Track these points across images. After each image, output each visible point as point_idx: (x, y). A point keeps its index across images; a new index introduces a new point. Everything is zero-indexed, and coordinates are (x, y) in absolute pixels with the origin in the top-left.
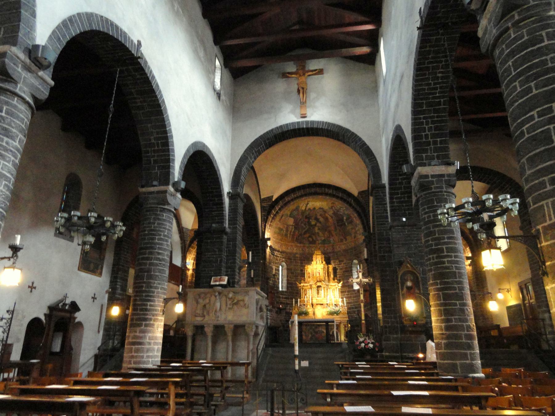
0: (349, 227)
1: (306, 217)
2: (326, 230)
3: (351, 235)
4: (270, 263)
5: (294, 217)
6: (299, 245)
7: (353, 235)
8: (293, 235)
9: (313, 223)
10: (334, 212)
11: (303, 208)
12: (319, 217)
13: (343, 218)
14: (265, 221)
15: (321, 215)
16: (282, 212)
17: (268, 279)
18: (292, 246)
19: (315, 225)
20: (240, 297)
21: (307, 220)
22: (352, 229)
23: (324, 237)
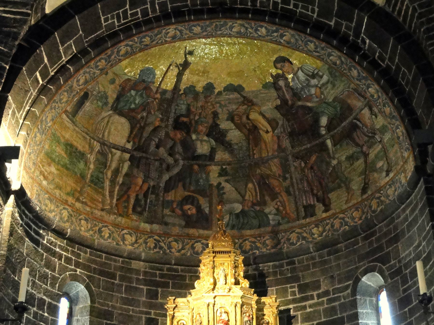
0: (340, 155)
1: (178, 125)
2: (248, 178)
3: (345, 183)
5: (129, 115)
6: (147, 227)
7: (356, 185)
8: (126, 188)
9: (203, 148)
10: (284, 101)
11: (169, 85)
12: (224, 125)
13: (317, 121)
15: (231, 118)
16: (81, 77)
18: (116, 225)
19: (211, 157)
21: (179, 135)
22: (351, 158)
23: (243, 201)
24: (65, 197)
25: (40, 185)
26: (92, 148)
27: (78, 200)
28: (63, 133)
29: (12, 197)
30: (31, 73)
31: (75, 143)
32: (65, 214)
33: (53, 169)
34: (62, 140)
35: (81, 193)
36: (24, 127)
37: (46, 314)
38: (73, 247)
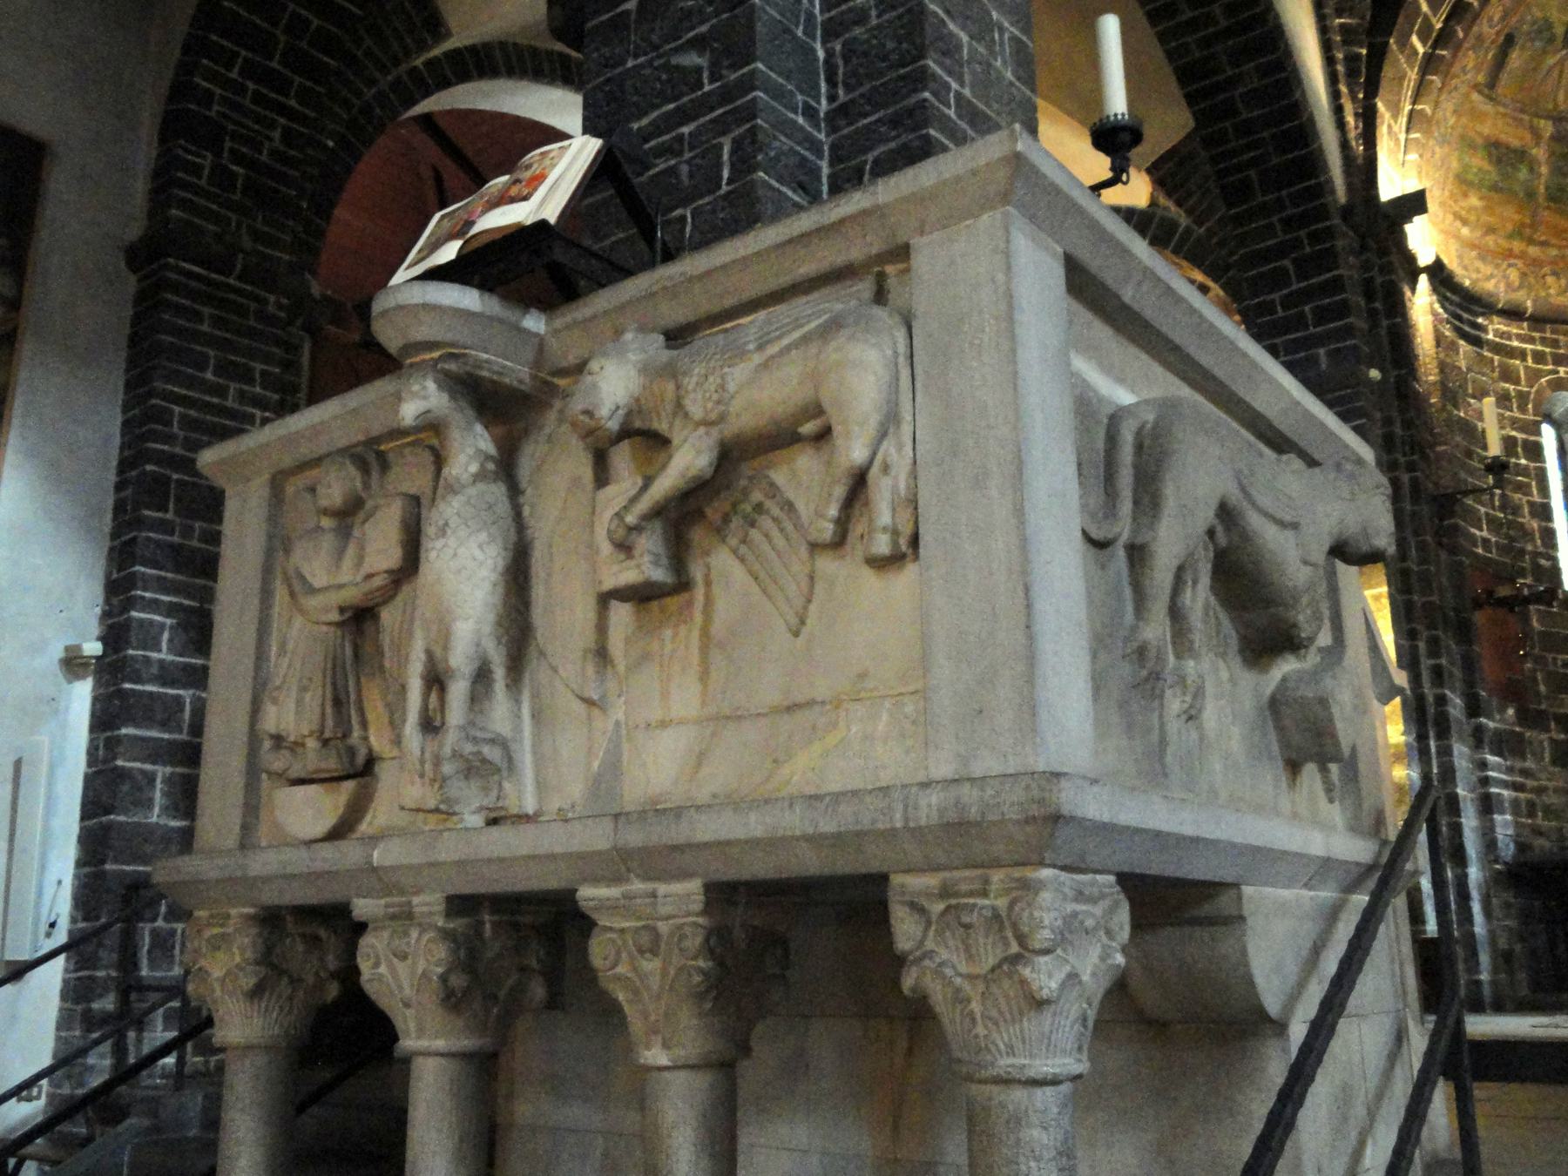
4: (1452, 396)
14: (1363, 73)
17: (1447, 504)
20: (747, 382)
24: (1504, 243)
25: (1457, 237)
26: (1536, 134)
27: (1531, 241)
28: (1479, 128)
29: (1423, 280)
30: (1404, 43)
31: (1503, 137)
32: (1514, 275)
33: (1474, 201)
34: (1479, 141)
35: (1533, 226)
36: (1411, 146)
37: (1523, 461)
38: (1543, 331)
